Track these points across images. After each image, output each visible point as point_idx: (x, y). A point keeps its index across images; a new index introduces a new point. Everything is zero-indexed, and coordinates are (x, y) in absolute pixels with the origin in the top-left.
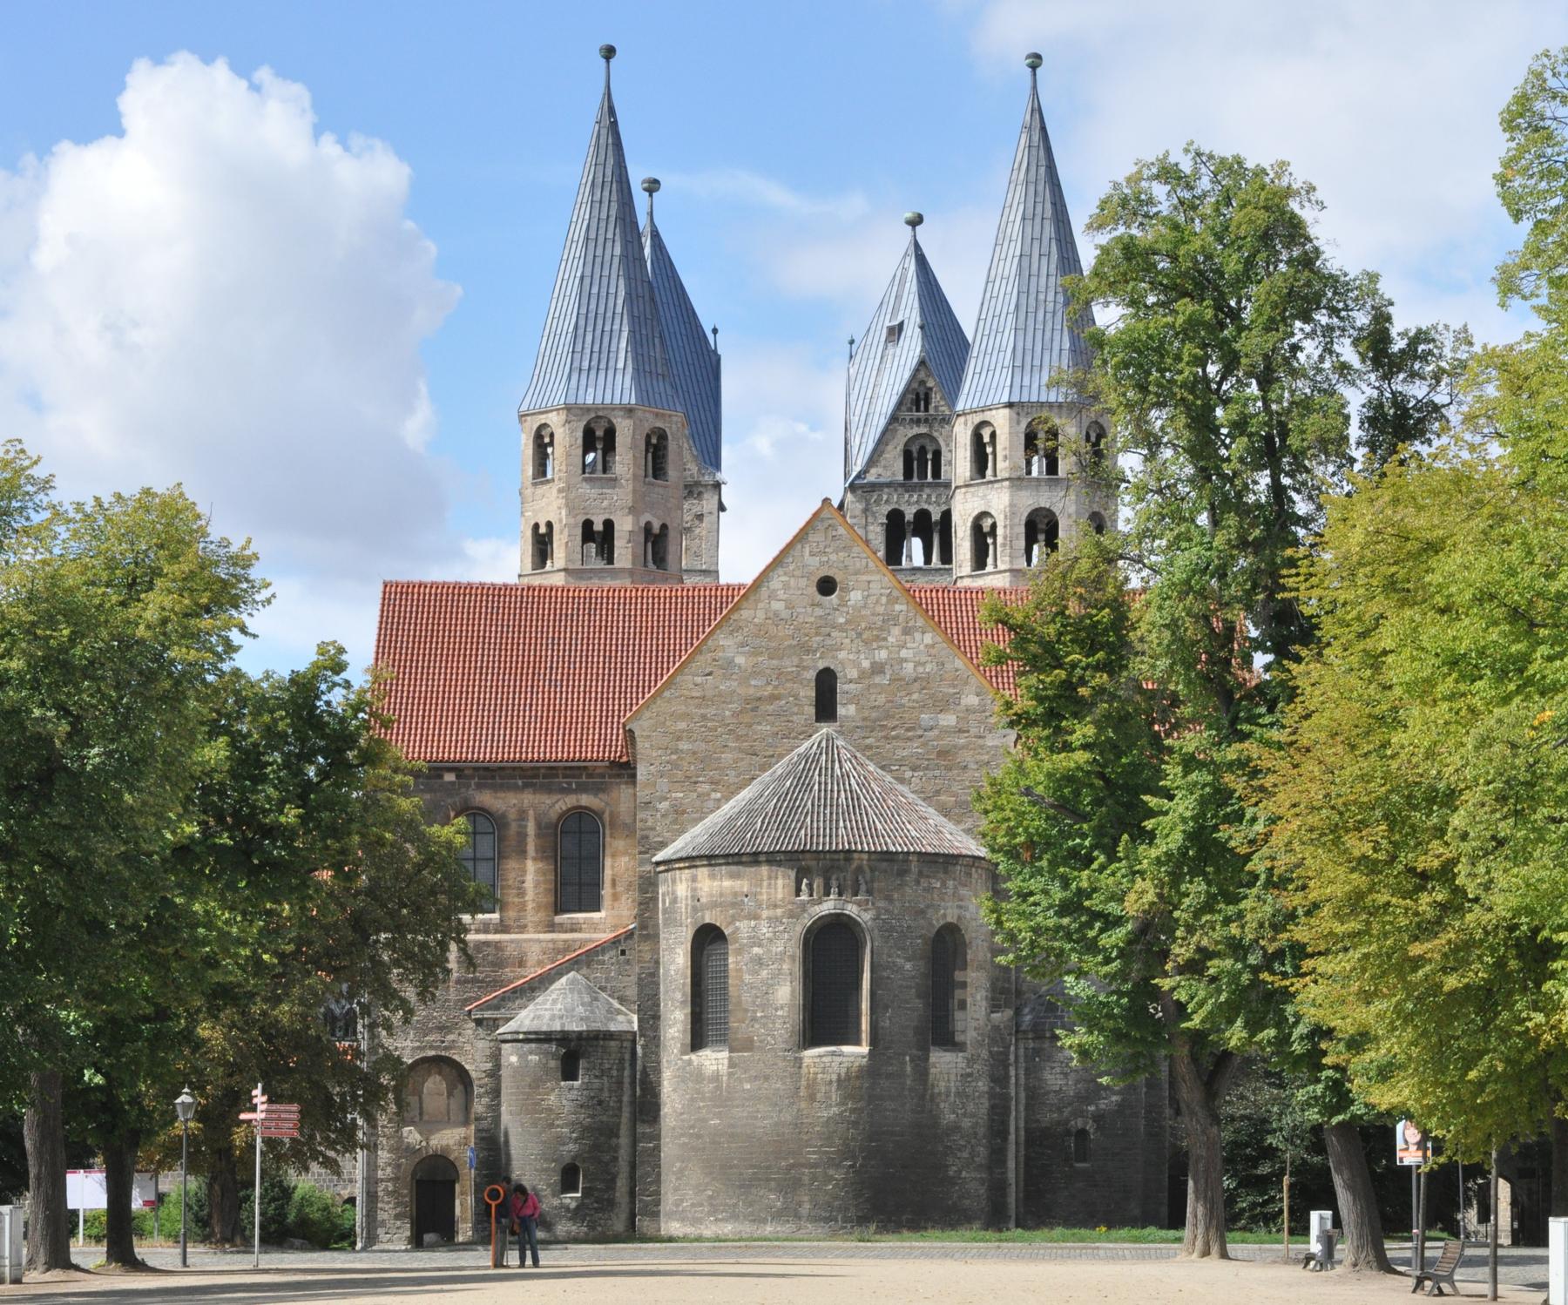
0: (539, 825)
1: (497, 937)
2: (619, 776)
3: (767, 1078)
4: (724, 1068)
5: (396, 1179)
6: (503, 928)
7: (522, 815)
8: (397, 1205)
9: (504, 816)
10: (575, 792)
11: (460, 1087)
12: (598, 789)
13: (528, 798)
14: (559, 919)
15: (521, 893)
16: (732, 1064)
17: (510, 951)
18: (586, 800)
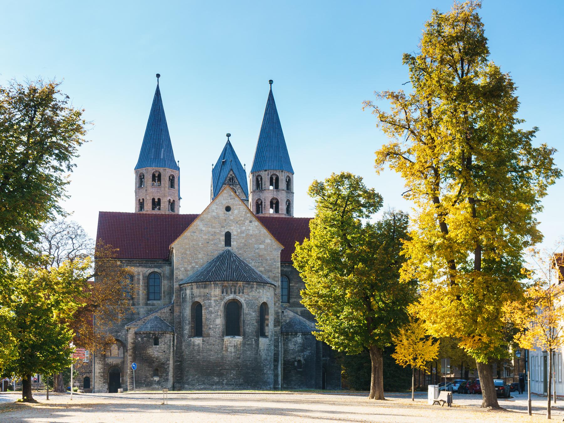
0: (143, 276)
3: (214, 345)
5: (103, 373)
8: (104, 379)
10: (153, 268)
12: (159, 267)
13: (140, 269)
15: (138, 294)
16: (203, 341)
18: (156, 270)
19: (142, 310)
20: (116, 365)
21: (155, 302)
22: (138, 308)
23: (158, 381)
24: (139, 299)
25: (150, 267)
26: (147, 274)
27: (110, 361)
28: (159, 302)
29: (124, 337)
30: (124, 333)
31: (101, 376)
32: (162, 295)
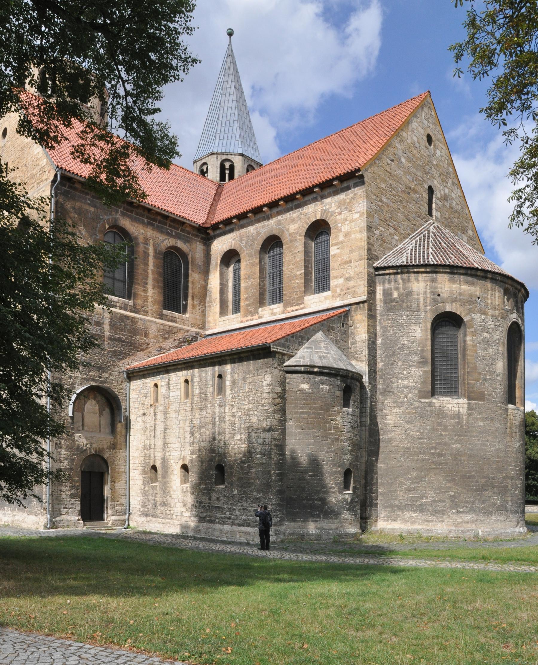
0: (155, 250)
2: (197, 236)
4: (464, 409)
6: (135, 310)
7: (146, 242)
9: (136, 238)
12: (187, 240)
14: (166, 312)
17: (140, 325)
24: (146, 299)
25: (170, 235)
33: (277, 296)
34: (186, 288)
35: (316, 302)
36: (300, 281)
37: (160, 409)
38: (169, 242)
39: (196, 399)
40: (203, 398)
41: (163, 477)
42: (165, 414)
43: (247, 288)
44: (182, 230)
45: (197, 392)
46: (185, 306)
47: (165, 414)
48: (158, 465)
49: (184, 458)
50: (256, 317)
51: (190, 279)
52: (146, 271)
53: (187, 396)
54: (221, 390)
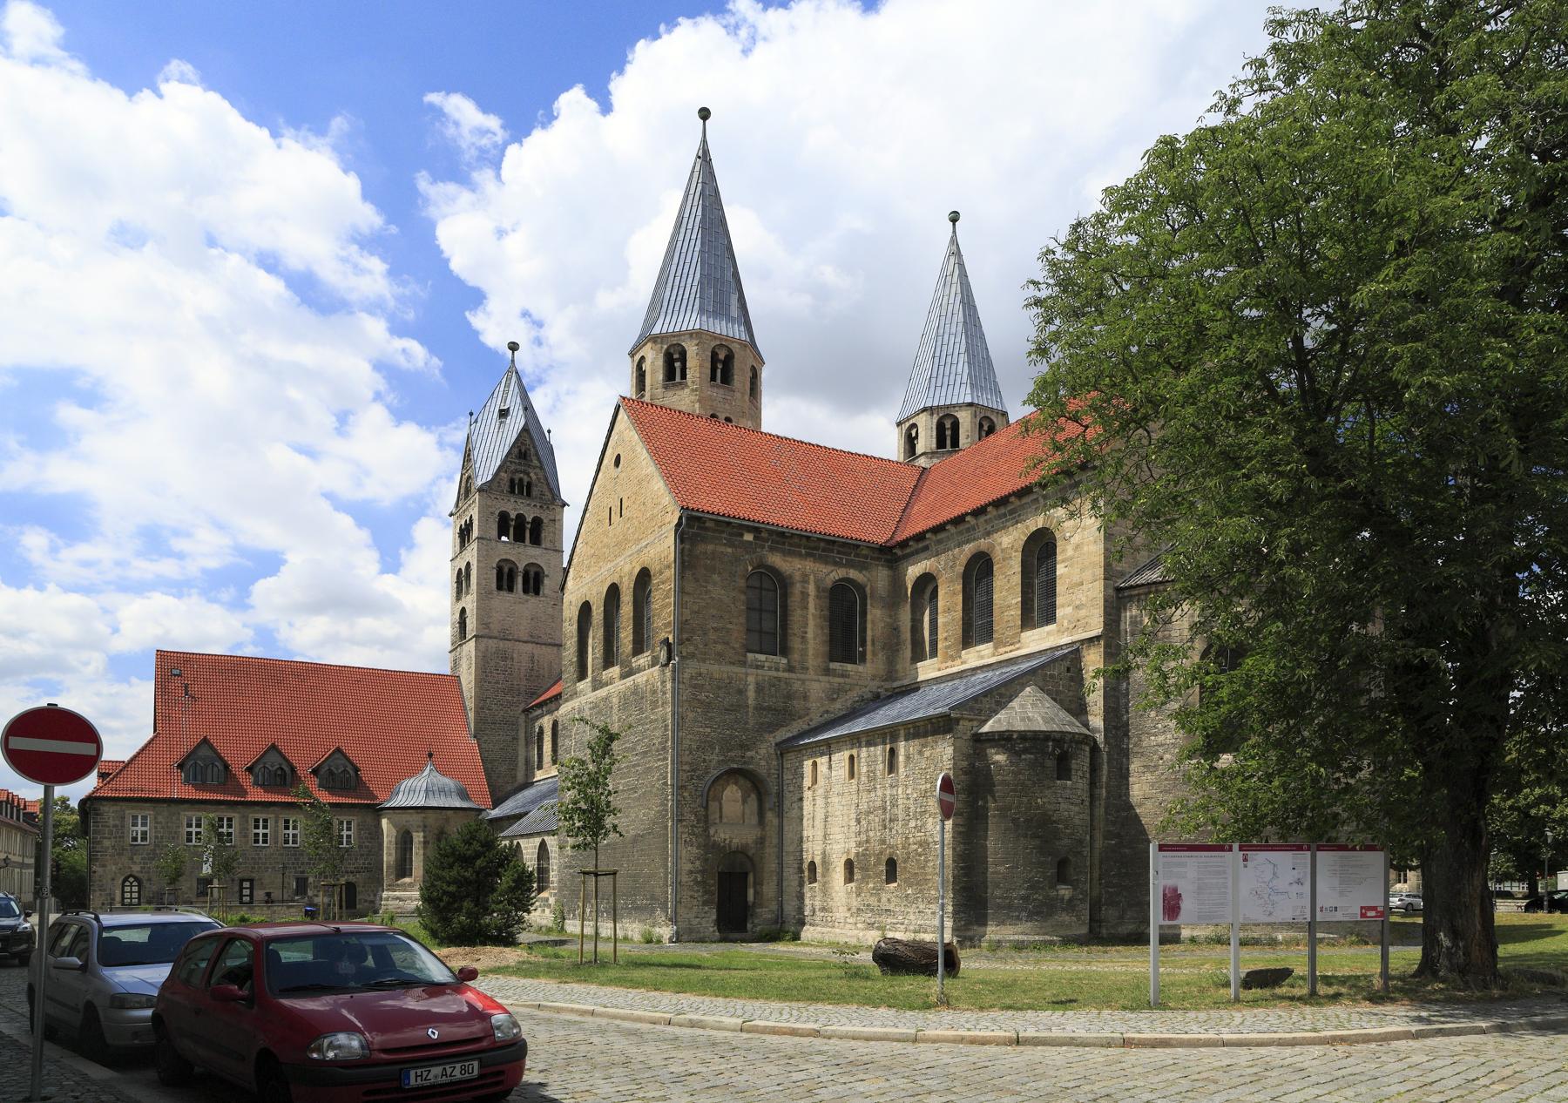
0: (818, 588)
1: (786, 675)
2: (878, 559)
5: (702, 872)
6: (790, 669)
7: (805, 580)
8: (706, 892)
9: (791, 576)
10: (844, 566)
11: (753, 796)
12: (862, 567)
13: (809, 565)
14: (833, 665)
15: (804, 639)
17: (797, 686)
18: (853, 574)
19: (815, 686)
20: (742, 852)
21: (849, 667)
22: (803, 681)
23: (1070, 900)
24: (804, 653)
26: (829, 583)
27: (722, 834)
28: (861, 668)
29: (763, 763)
30: (763, 751)
31: (697, 883)
32: (869, 647)
33: (987, 635)
34: (864, 630)
35: (1038, 640)
36: (1016, 612)
37: (820, 792)
38: (838, 573)
39: (863, 779)
40: (872, 777)
41: (824, 876)
42: (826, 798)
43: (945, 624)
44: (857, 555)
45: (864, 770)
46: (863, 654)
47: (826, 798)
48: (818, 860)
49: (848, 852)
50: (958, 662)
51: (869, 617)
52: (805, 617)
53: (852, 775)
54: (892, 767)
